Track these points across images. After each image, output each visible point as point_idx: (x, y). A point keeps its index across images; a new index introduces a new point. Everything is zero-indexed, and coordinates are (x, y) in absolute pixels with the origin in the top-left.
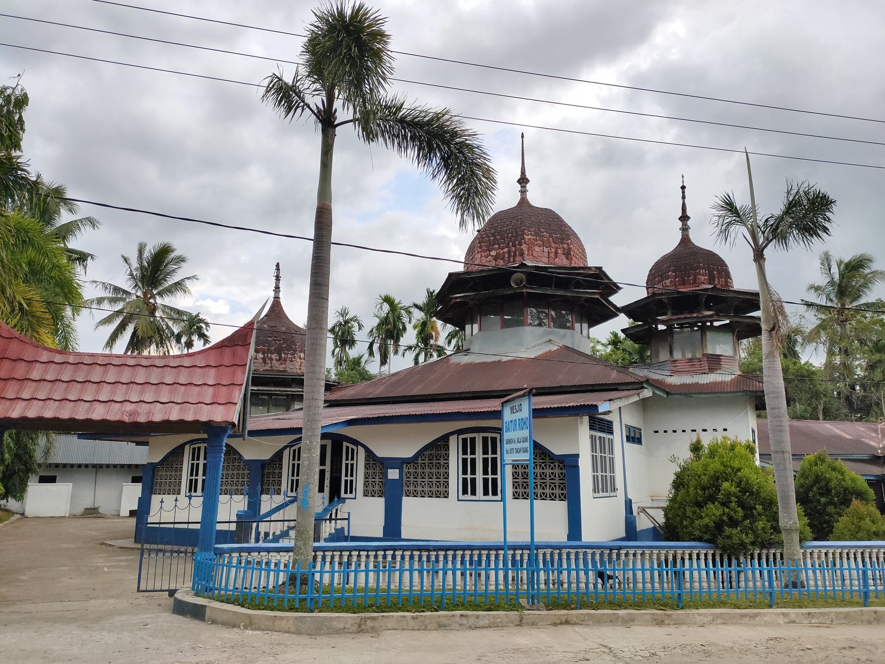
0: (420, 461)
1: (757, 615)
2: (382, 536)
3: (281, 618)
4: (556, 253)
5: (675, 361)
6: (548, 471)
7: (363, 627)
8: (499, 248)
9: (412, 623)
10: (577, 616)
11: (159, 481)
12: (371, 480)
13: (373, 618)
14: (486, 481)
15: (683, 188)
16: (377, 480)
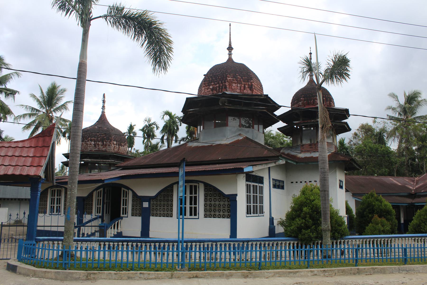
0: (159, 198)
1: (297, 272)
2: (140, 236)
3: (48, 272)
4: (244, 87)
5: (303, 145)
6: (222, 203)
7: (89, 277)
8: (214, 84)
9: (114, 276)
10: (202, 274)
12: (135, 208)
13: (94, 274)
14: (191, 208)
16: (138, 208)
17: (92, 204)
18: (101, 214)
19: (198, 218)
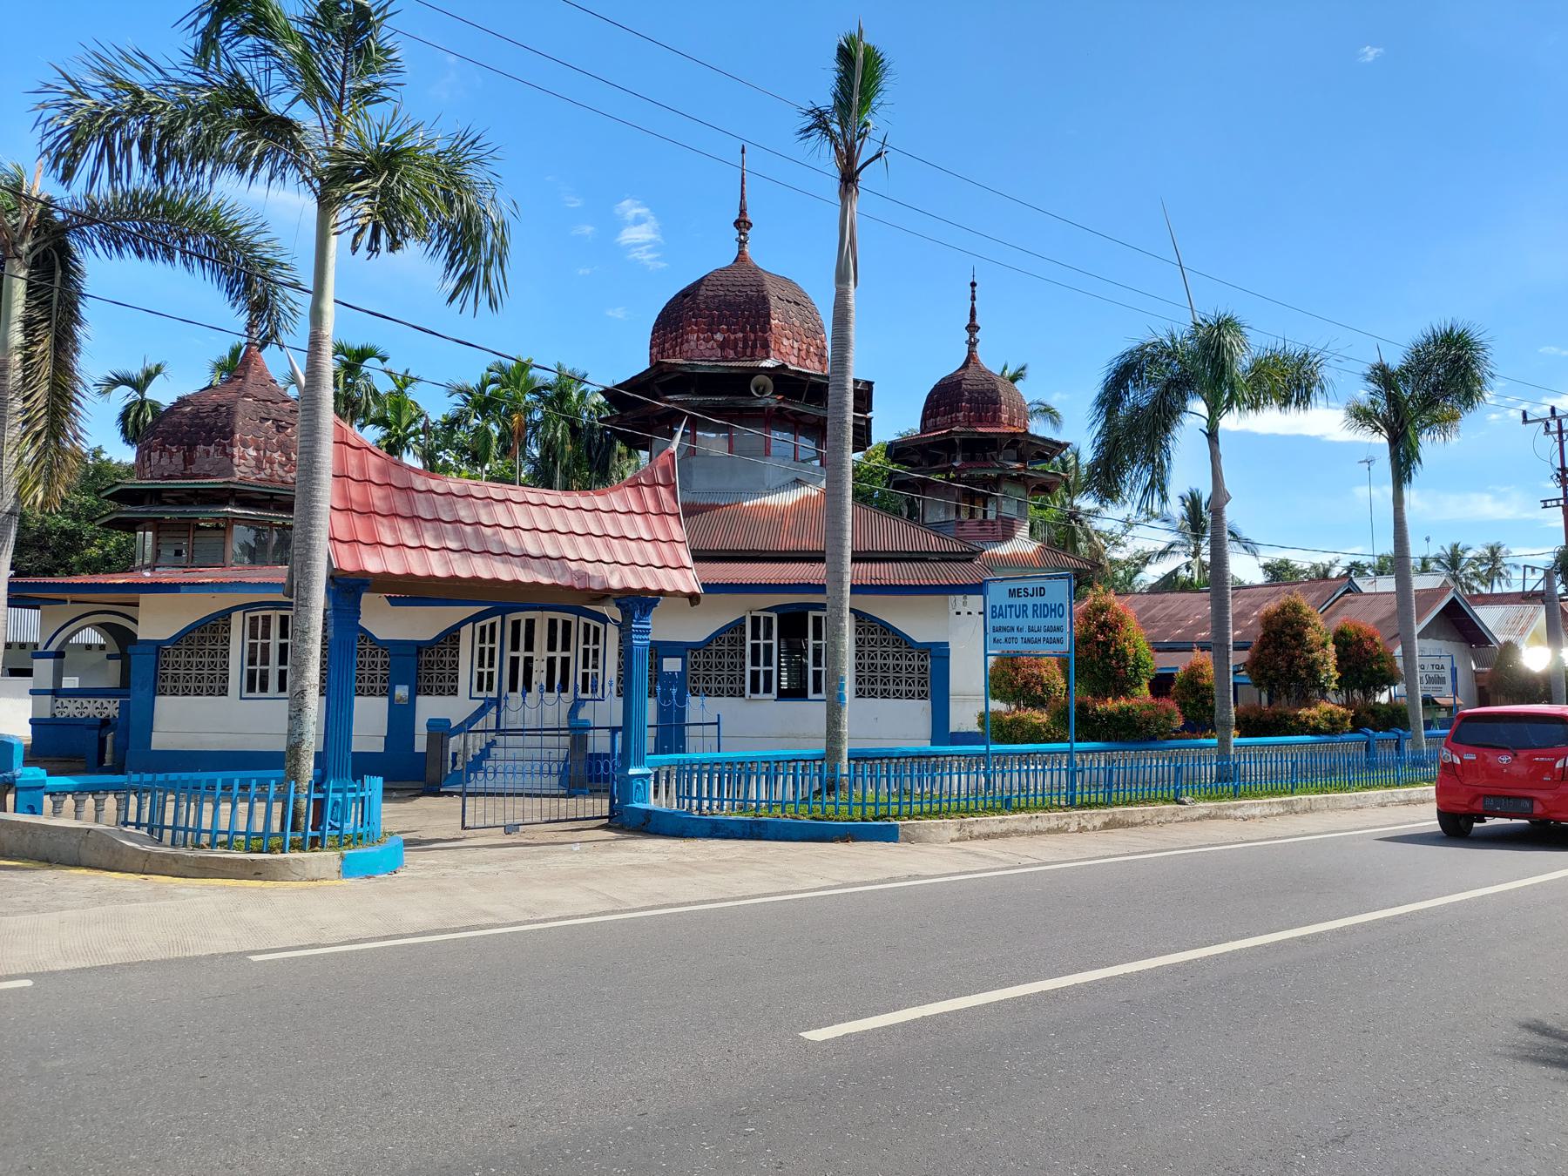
0: (714, 647)
4: (808, 351)
8: (729, 330)
11: (170, 671)
15: (973, 285)
17: (455, 665)
18: (494, 694)
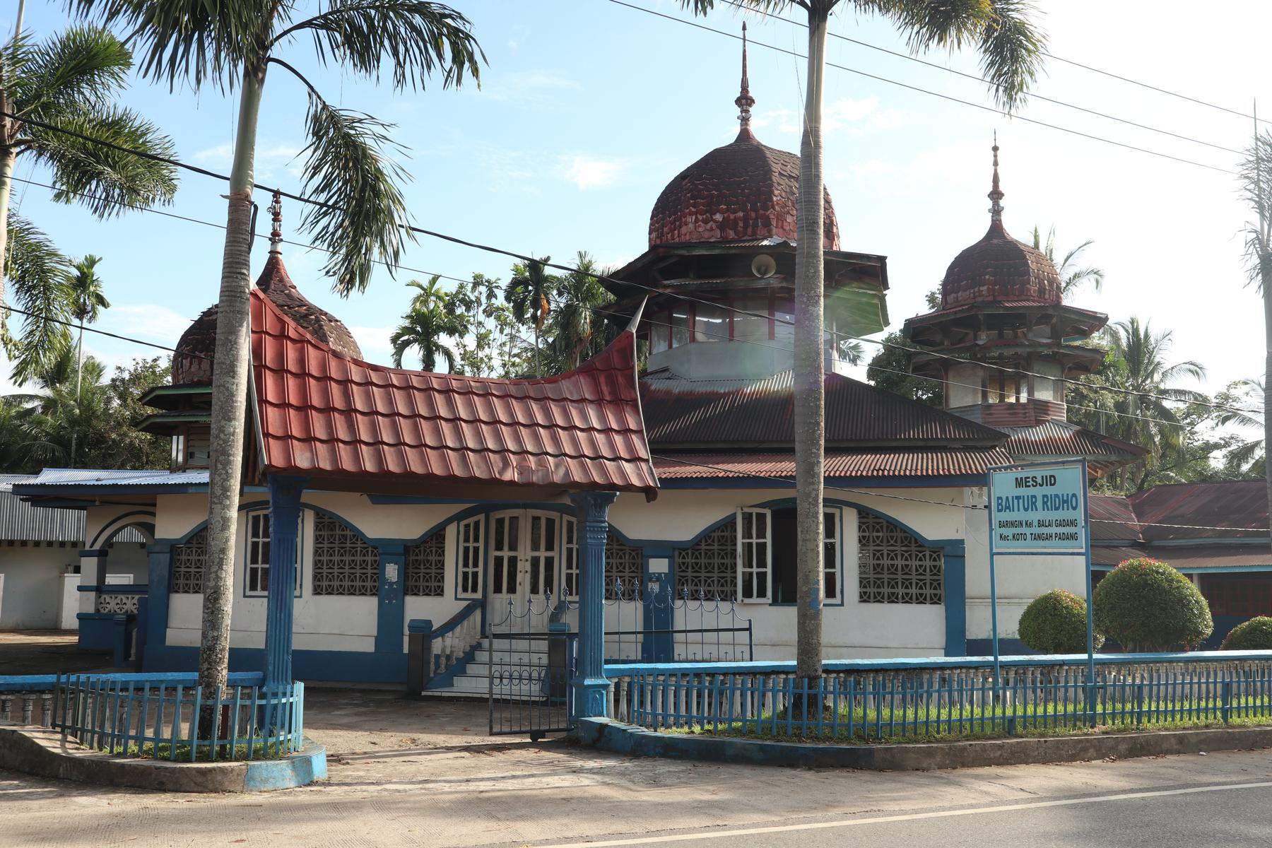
0: (703, 547)
2: (639, 657)
8: (728, 210)
11: (183, 570)
15: (995, 149)
17: (441, 565)
18: (479, 595)
19: (842, 604)
